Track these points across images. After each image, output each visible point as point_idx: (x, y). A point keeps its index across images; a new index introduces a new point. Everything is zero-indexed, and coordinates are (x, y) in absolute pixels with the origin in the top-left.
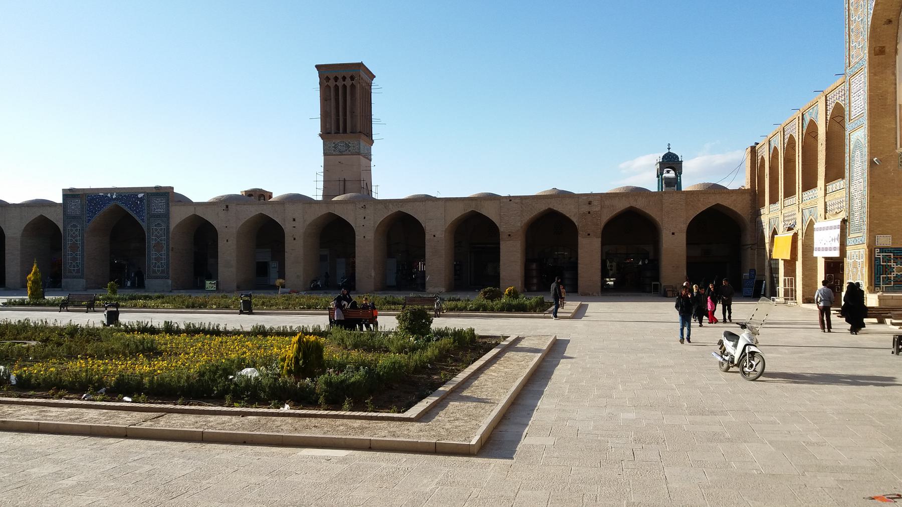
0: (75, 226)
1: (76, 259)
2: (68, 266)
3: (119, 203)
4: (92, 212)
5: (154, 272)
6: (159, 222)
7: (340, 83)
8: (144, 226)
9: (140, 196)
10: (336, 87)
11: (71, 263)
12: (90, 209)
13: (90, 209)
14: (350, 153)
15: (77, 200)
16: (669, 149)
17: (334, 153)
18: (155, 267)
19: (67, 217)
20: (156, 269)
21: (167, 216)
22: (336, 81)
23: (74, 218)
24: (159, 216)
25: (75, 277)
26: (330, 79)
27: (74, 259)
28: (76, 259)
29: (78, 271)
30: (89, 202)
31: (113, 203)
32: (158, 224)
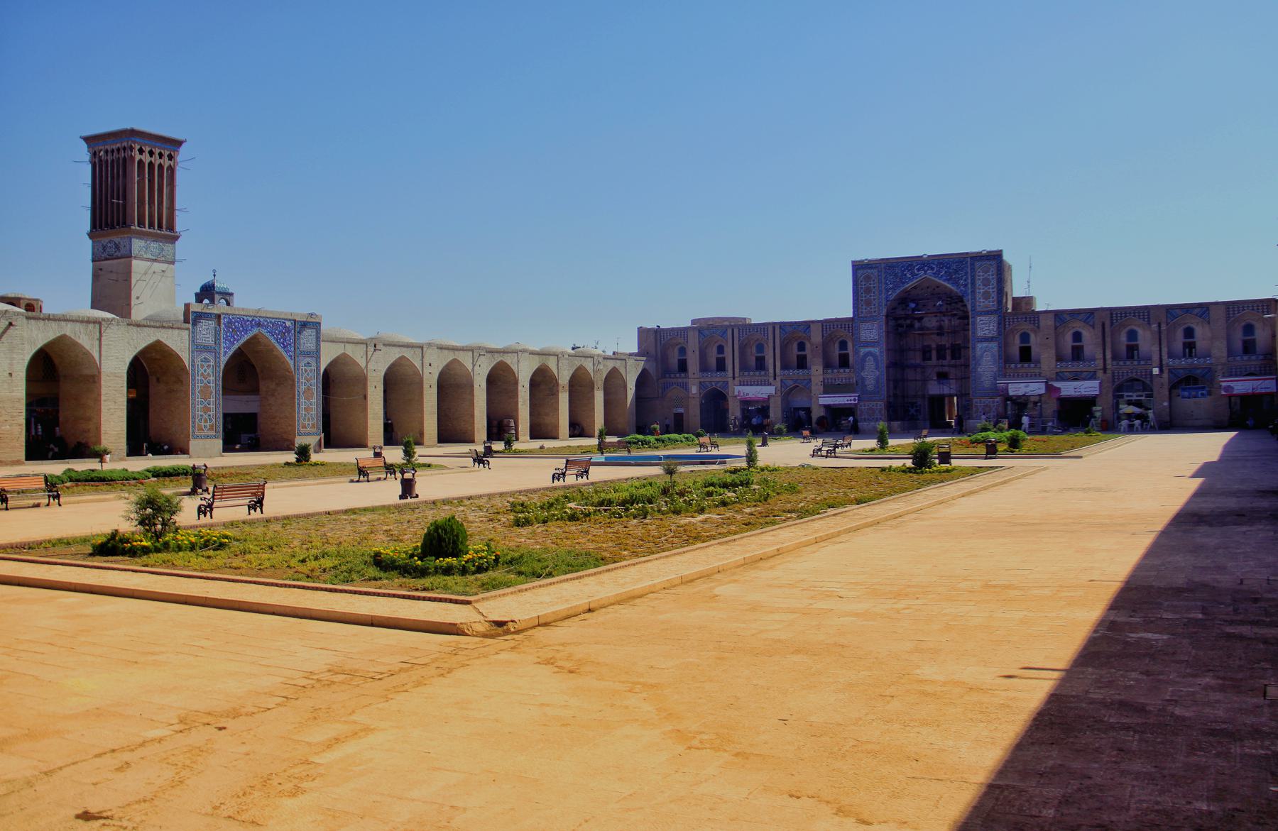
0: (206, 360)
1: (209, 410)
2: (197, 420)
3: (263, 331)
4: (230, 341)
5: (304, 427)
6: (308, 360)
7: (157, 161)
8: (291, 363)
9: (288, 324)
10: (151, 164)
11: (202, 415)
12: (227, 336)
13: (226, 335)
14: (163, 259)
15: (210, 322)
16: (214, 276)
17: (145, 256)
18: (304, 420)
19: (197, 348)
20: (306, 422)
21: (317, 354)
22: (151, 156)
23: (206, 349)
24: (307, 354)
25: (208, 437)
26: (144, 152)
27: (206, 410)
28: (209, 410)
29: (211, 428)
30: (225, 326)
31: (256, 331)
32: (308, 363)
